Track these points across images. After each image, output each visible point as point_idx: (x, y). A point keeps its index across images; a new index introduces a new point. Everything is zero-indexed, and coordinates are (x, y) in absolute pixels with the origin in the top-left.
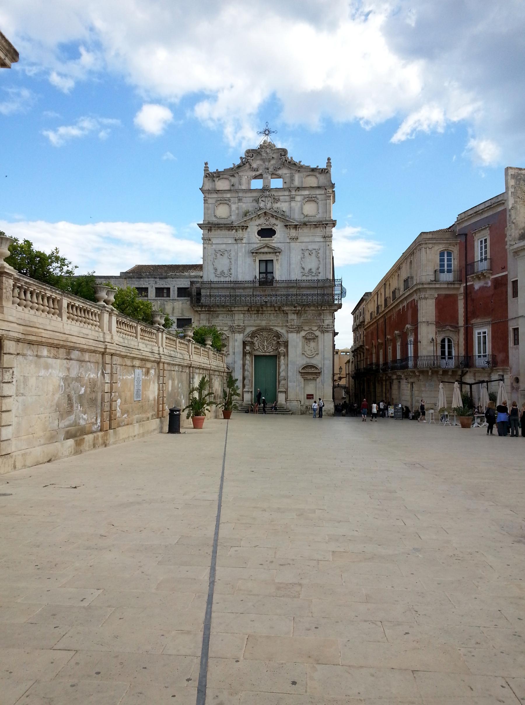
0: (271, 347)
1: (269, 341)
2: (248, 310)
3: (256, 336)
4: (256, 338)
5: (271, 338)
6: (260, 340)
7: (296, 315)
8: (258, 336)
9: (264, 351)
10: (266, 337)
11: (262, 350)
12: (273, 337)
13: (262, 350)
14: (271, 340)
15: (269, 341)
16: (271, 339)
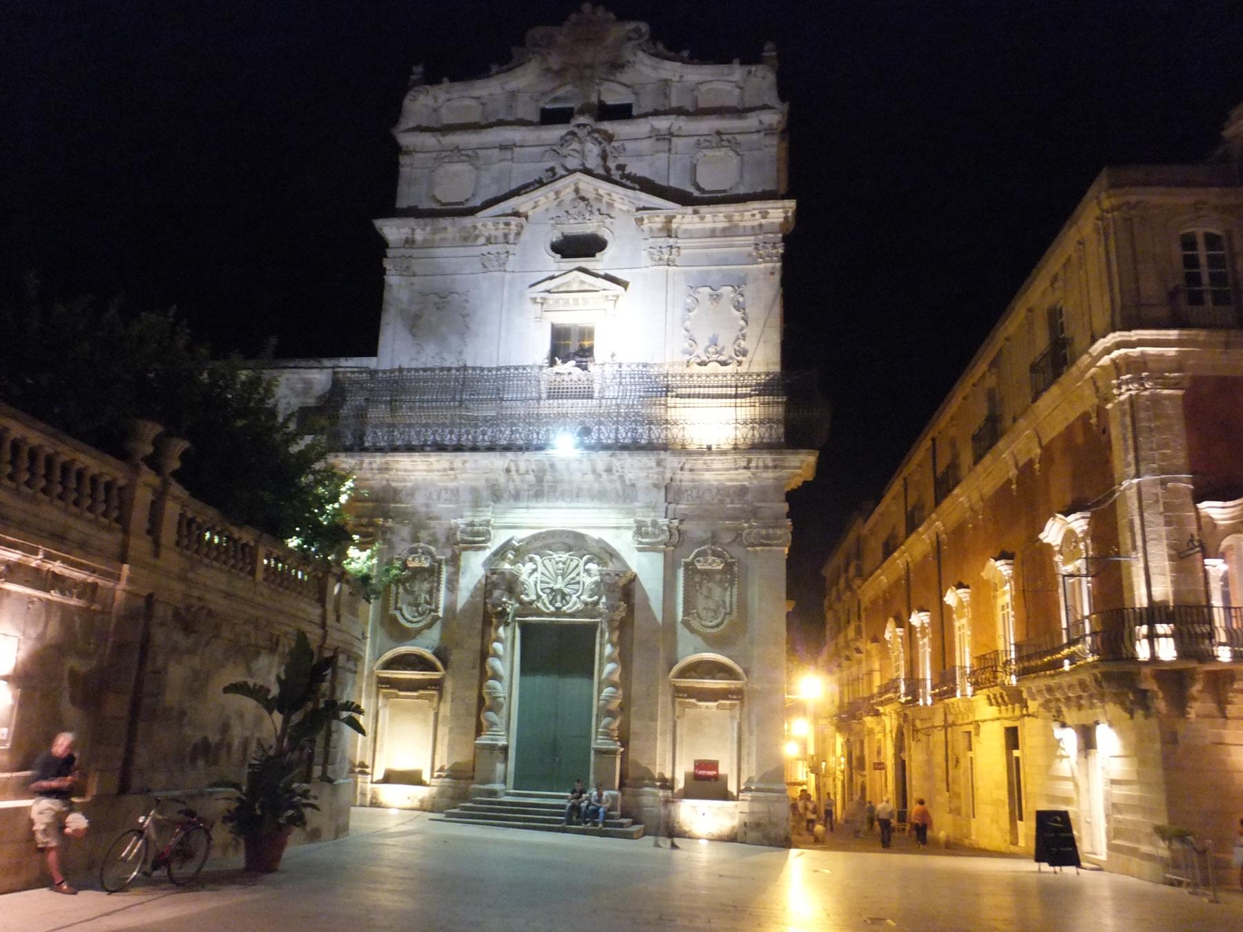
0: (578, 597)
1: (573, 575)
2: (508, 471)
3: (531, 560)
4: (530, 566)
5: (577, 566)
6: (542, 573)
7: (663, 492)
8: (537, 558)
9: (552, 609)
10: (564, 563)
11: (548, 604)
12: (586, 563)
13: (548, 604)
14: (578, 574)
15: (573, 575)
16: (576, 571)
